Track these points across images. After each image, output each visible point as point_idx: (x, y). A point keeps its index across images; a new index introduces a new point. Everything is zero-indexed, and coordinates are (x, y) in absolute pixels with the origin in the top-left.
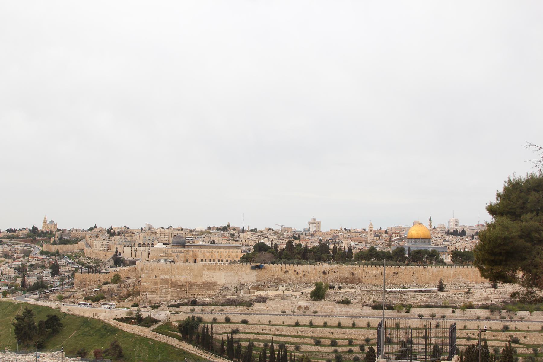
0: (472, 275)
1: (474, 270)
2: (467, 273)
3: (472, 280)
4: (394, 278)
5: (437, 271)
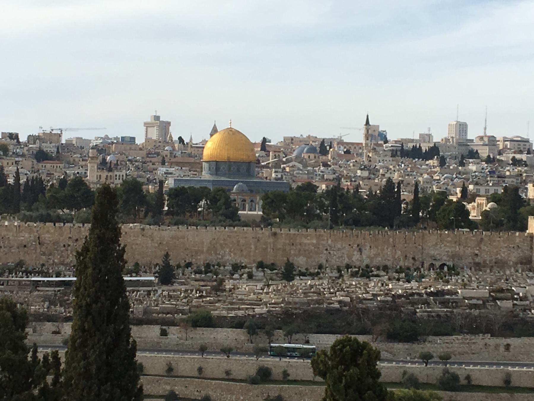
0: (253, 247)
3: (252, 258)
4: (69, 252)
5: (173, 238)
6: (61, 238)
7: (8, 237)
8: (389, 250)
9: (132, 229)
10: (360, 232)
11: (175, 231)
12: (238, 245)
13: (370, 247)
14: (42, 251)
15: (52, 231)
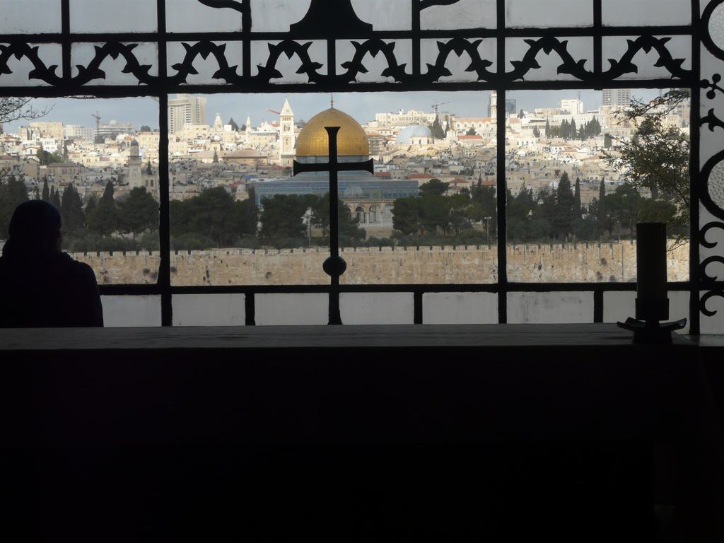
0: (394, 273)
1: (401, 257)
2: (377, 266)
6: (135, 272)
8: (578, 270)
10: (537, 247)
12: (374, 271)
13: (552, 267)
15: (122, 263)
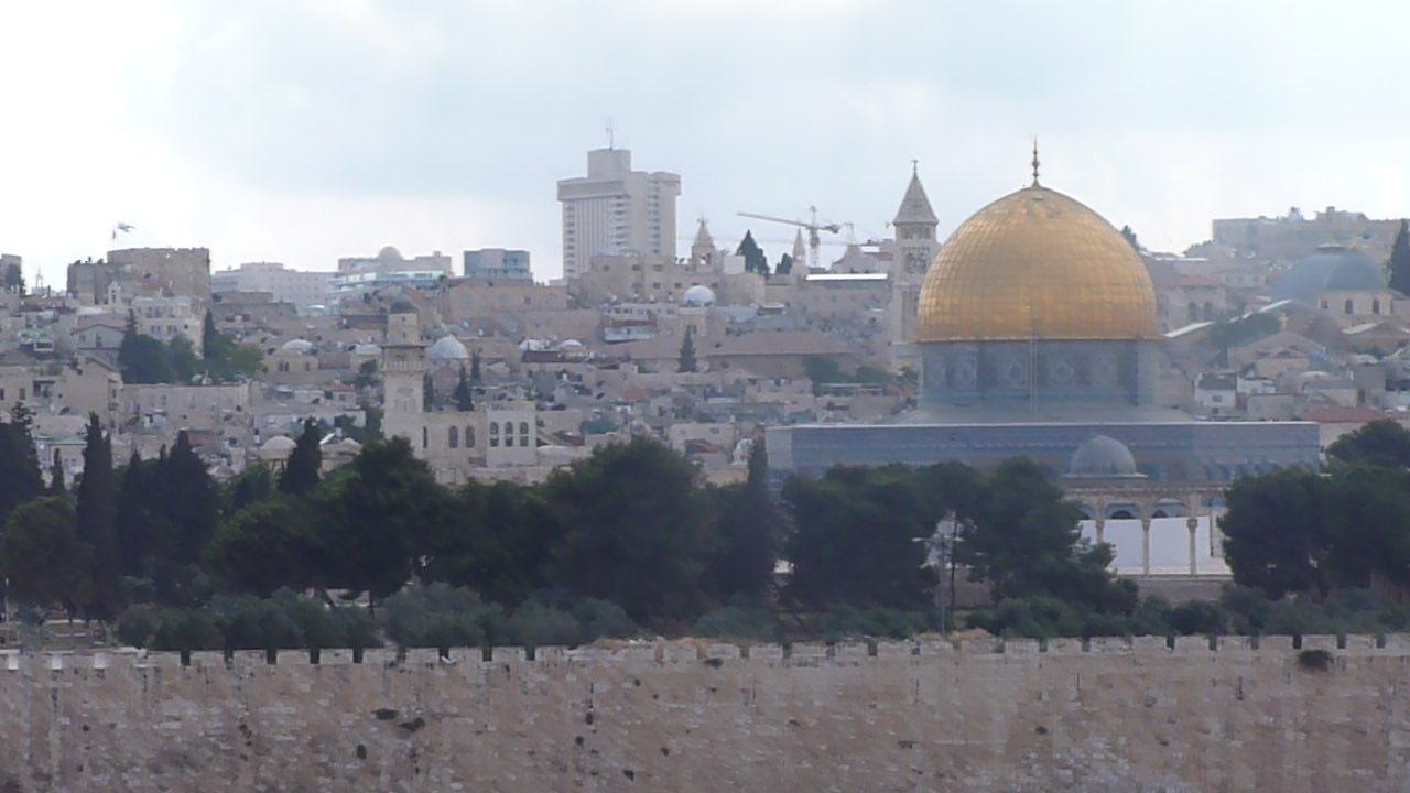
0: (1215, 725)
2: (1160, 703)
4: (384, 779)
6: (347, 719)
7: (105, 721)
9: (662, 663)
11: (856, 664)
14: (264, 782)
15: (306, 688)
